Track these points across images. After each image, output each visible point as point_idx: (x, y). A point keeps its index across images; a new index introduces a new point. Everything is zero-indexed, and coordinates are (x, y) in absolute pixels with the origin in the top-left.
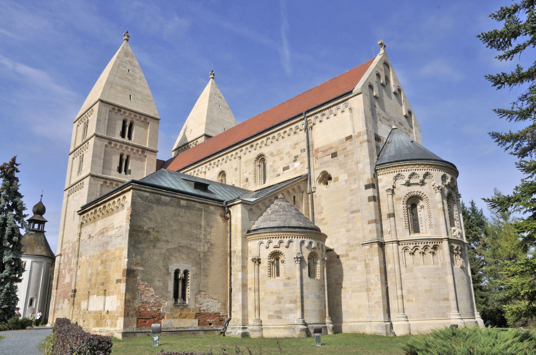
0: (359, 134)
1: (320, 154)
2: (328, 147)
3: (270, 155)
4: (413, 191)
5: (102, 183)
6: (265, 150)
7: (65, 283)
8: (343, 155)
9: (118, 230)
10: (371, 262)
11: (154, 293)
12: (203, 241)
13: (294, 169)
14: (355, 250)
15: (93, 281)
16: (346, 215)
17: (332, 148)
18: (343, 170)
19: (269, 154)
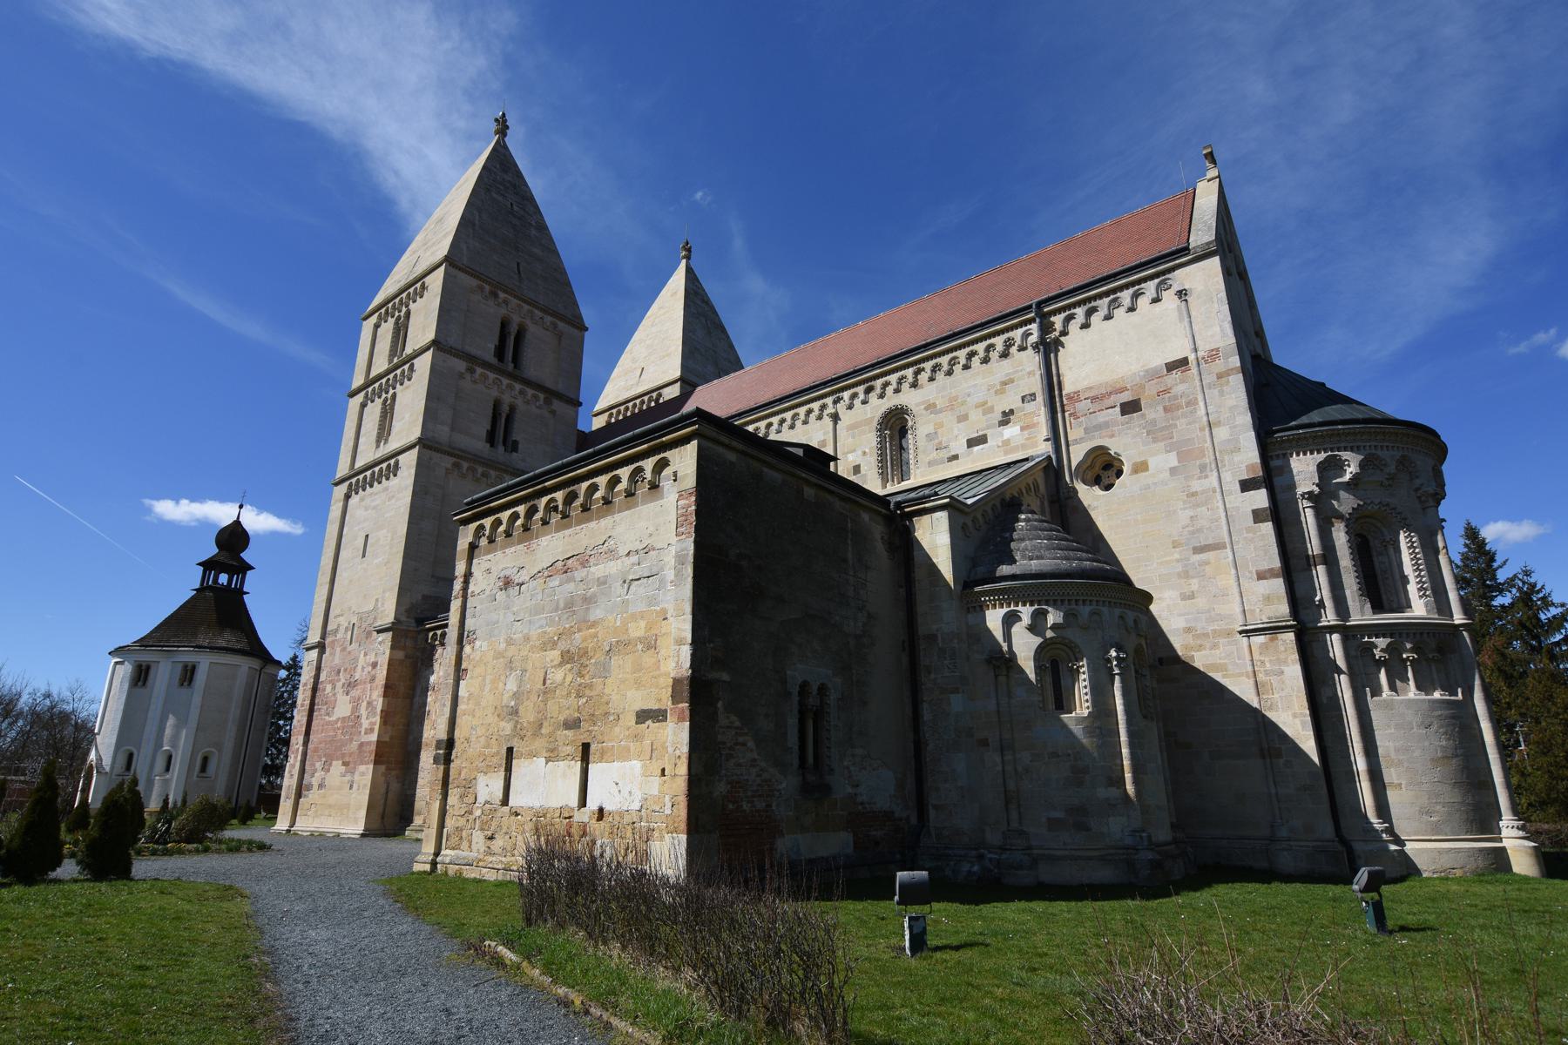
0: (1214, 355)
1: (1083, 406)
2: (1109, 390)
3: (926, 409)
4: (1369, 502)
5: (449, 466)
6: (908, 398)
7: (334, 718)
8: (1160, 408)
9: (634, 559)
10: (1274, 680)
13: (1003, 442)
14: (1215, 646)
15: (528, 715)
16: (1177, 556)
17: (1122, 390)
18: (1163, 444)
19: (923, 407)
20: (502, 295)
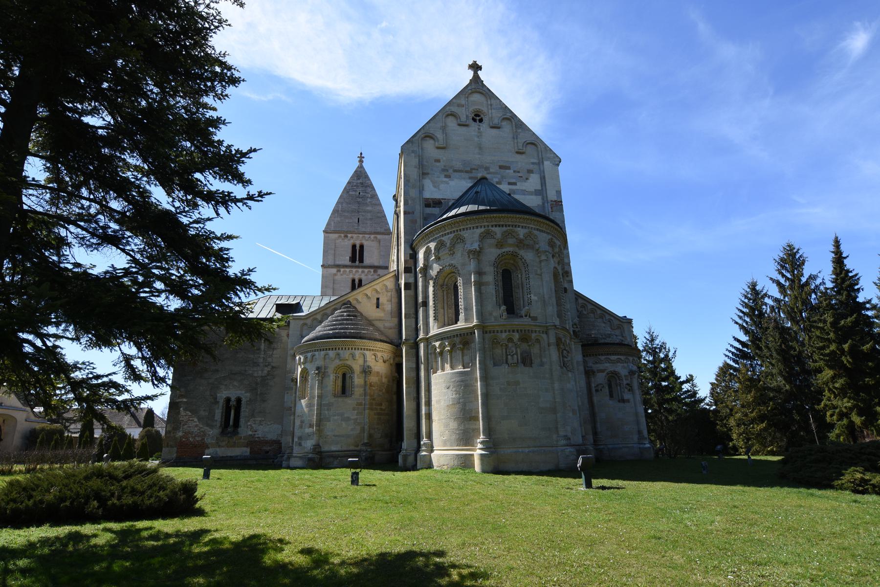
4: (444, 266)
11: (198, 423)
12: (261, 365)
20: (349, 235)
